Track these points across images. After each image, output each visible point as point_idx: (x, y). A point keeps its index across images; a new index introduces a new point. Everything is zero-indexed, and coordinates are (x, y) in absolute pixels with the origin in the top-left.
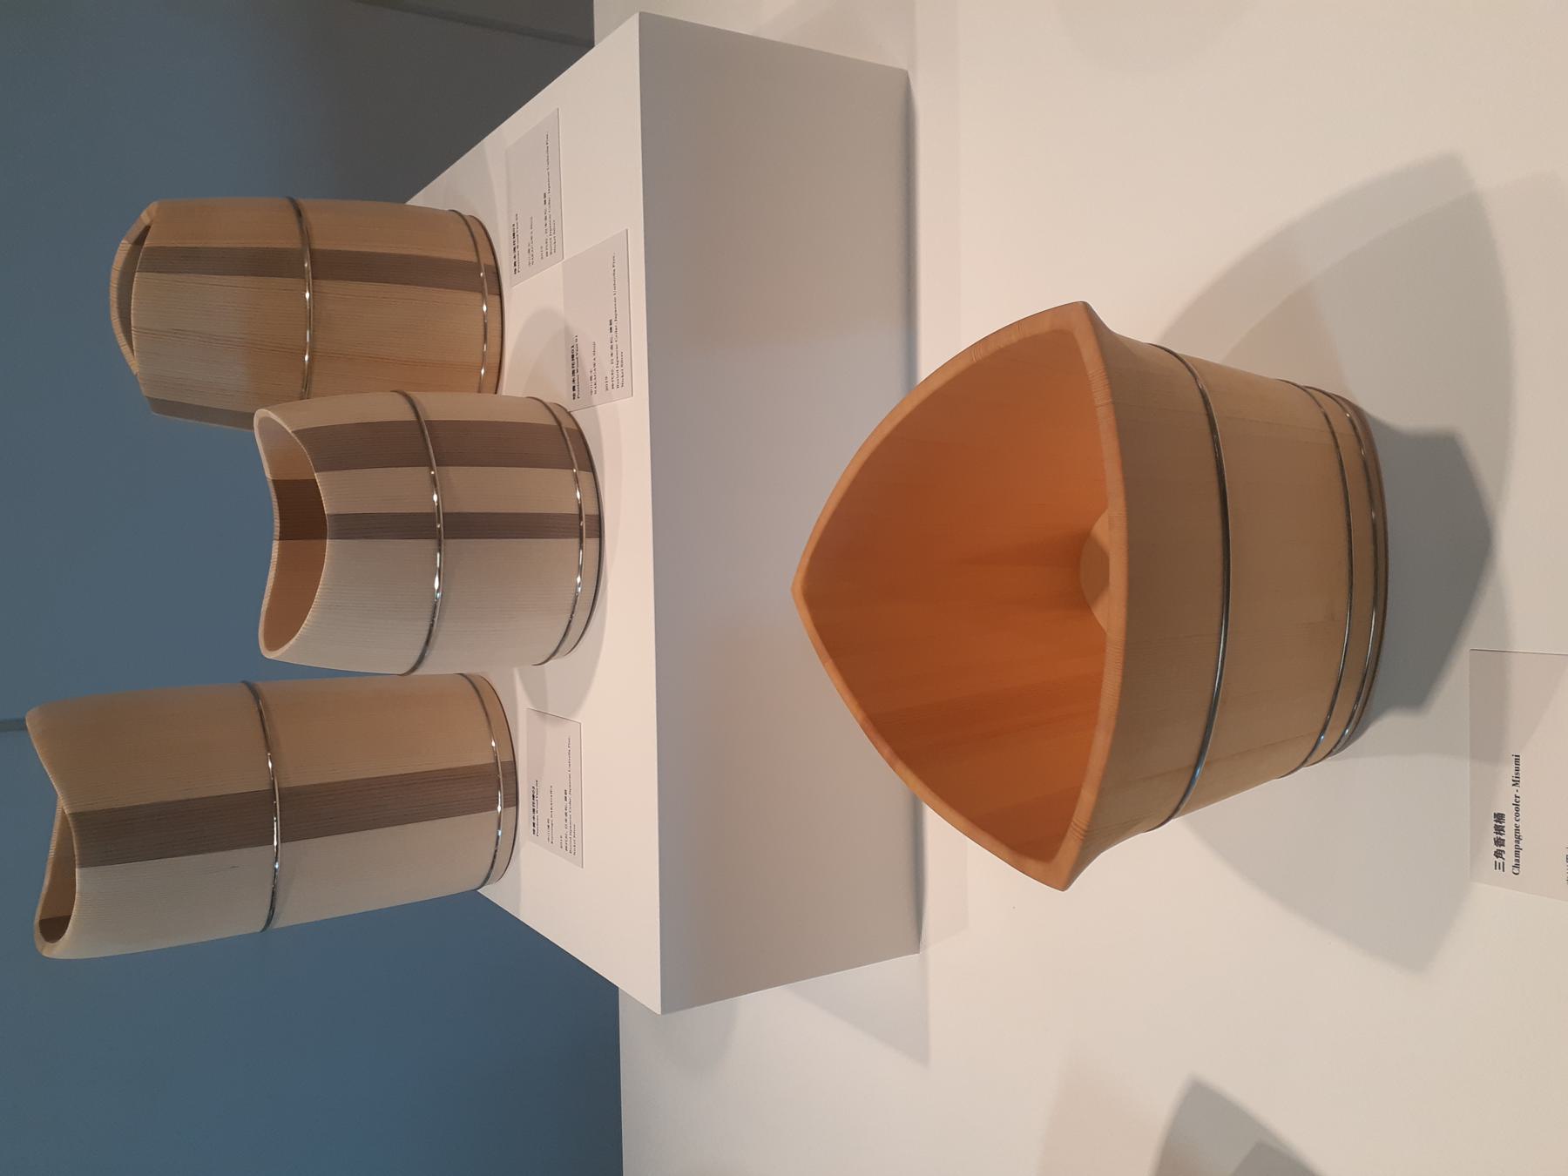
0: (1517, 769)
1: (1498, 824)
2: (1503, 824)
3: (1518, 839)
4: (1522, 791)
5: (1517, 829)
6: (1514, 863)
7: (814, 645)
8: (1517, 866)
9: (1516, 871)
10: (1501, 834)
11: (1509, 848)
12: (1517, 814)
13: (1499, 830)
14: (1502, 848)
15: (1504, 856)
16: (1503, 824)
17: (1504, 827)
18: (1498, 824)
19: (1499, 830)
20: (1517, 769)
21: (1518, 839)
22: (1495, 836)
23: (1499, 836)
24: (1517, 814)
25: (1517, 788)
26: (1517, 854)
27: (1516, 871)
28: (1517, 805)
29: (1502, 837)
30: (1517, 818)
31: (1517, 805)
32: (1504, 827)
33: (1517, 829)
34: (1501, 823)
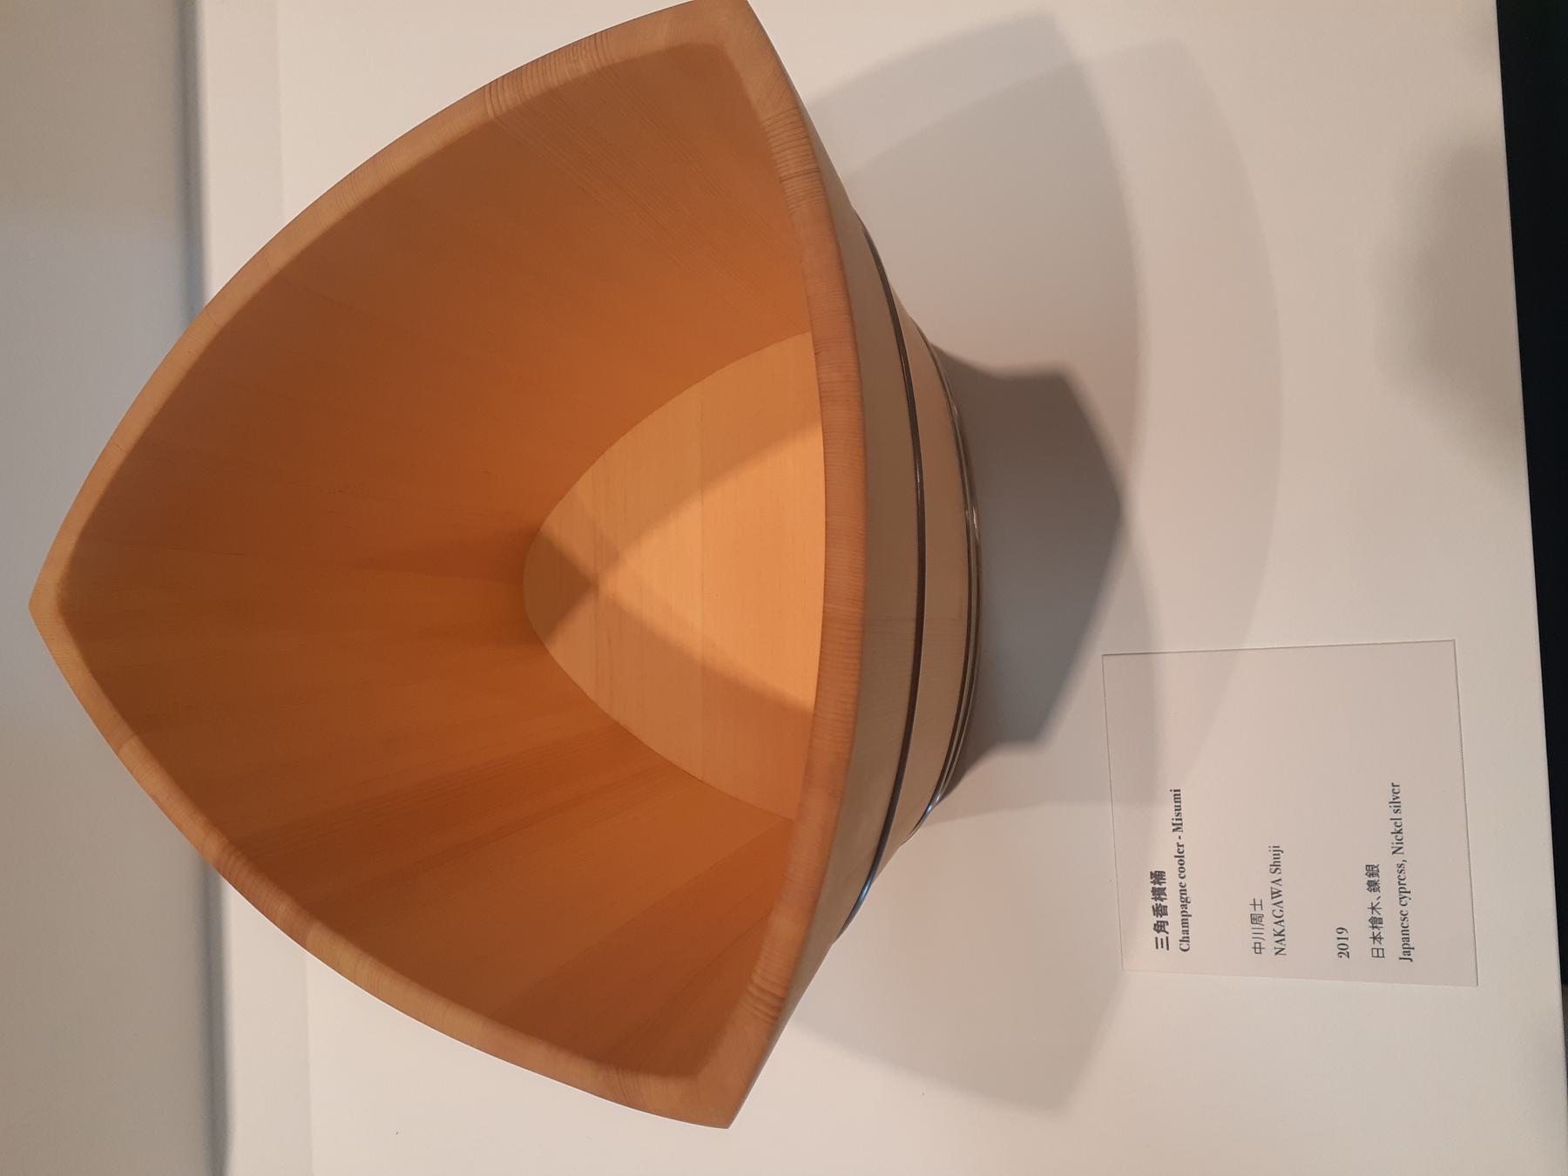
0: (1178, 809)
1: (1157, 886)
2: (1163, 886)
3: (1185, 902)
4: (1187, 836)
5: (1183, 891)
6: (1181, 936)
7: (78, 696)
8: (1185, 940)
9: (1185, 946)
10: (1162, 900)
11: (1173, 918)
12: (1182, 869)
13: (1158, 893)
14: (1164, 918)
15: (1167, 928)
16: (1163, 886)
17: (1165, 889)
18: (1157, 886)
19: (1158, 893)
20: (1178, 809)
21: (1185, 902)
22: (1154, 902)
23: (1158, 902)
24: (1182, 869)
25: (1180, 834)
26: (1185, 923)
27: (1185, 946)
28: (1180, 856)
29: (1163, 904)
30: (1182, 875)
31: (1180, 856)
32: (1165, 889)
33: (1183, 891)
34: (1160, 884)
